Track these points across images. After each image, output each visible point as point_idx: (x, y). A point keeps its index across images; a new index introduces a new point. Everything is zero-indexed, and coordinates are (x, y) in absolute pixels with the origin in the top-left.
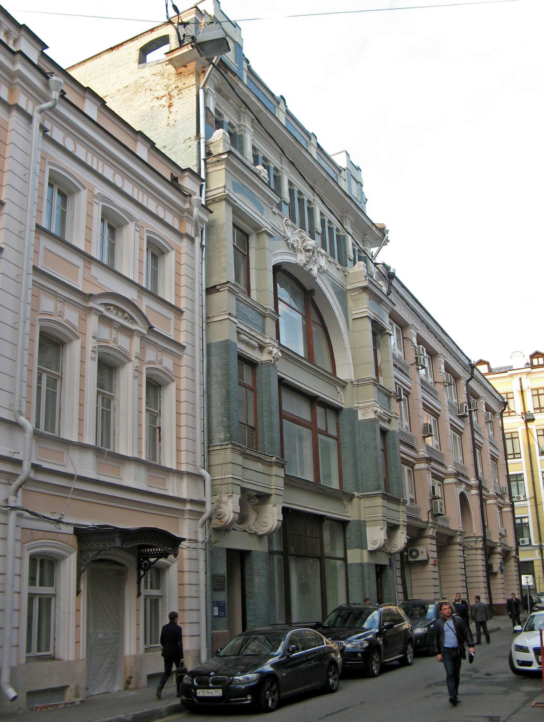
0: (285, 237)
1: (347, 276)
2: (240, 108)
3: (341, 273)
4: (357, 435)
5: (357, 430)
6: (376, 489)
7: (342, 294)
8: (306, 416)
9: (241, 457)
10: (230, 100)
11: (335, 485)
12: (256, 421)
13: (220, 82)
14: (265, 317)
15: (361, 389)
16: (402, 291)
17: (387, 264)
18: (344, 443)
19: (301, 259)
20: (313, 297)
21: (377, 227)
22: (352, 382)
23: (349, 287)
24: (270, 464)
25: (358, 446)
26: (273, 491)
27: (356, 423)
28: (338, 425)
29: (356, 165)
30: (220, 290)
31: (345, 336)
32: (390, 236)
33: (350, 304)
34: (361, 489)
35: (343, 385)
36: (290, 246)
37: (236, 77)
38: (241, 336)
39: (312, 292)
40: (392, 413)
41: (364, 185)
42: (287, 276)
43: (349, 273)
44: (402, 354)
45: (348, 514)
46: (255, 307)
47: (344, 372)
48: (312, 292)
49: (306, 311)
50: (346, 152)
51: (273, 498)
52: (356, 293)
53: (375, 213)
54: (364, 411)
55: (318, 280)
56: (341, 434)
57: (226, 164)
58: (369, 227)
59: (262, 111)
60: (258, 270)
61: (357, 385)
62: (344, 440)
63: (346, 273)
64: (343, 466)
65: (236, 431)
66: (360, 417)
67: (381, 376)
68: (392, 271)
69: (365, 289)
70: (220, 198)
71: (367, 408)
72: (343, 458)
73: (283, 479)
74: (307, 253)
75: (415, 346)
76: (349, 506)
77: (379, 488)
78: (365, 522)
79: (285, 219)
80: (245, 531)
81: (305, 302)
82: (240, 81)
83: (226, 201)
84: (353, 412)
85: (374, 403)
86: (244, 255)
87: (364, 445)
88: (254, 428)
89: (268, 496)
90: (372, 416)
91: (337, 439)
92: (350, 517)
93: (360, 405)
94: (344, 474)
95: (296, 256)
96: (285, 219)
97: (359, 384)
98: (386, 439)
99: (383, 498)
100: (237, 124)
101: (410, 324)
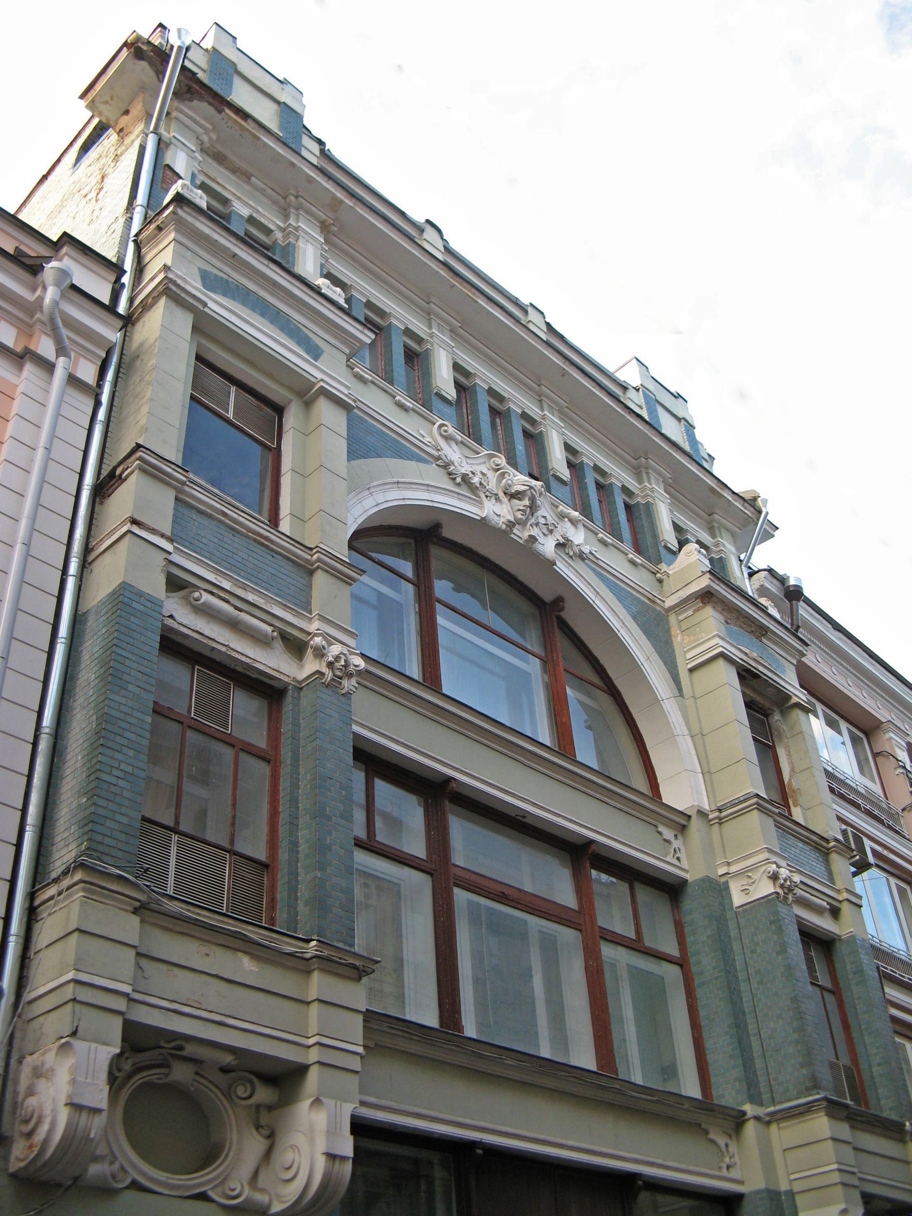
0: (438, 458)
1: (665, 583)
2: (285, 198)
3: (646, 575)
4: (736, 947)
5: (734, 933)
6: (807, 1089)
7: (655, 623)
8: (564, 893)
9: (136, 920)
10: (253, 179)
11: (691, 1088)
12: (273, 844)
13: (214, 136)
14: (311, 573)
15: (728, 827)
16: (839, 639)
17: (781, 571)
18: (701, 973)
19: (498, 512)
20: (562, 614)
21: (734, 493)
22: (701, 813)
23: (670, 602)
24: (302, 966)
25: (741, 976)
26: (313, 1055)
27: (729, 915)
28: (679, 927)
29: (672, 391)
30: (123, 476)
31: (671, 707)
32: (773, 512)
33: (678, 639)
34: (766, 1096)
35: (681, 823)
36: (459, 480)
37: (249, 121)
38: (196, 595)
39: (558, 602)
40: (838, 891)
41: (695, 424)
42: (477, 563)
43: (668, 575)
44: (877, 789)
45: (735, 1174)
46: (267, 538)
47: (682, 790)
48: (558, 602)
49: (546, 648)
50: (637, 359)
51: (313, 1075)
52: (690, 612)
53: (734, 471)
54: (745, 881)
55: (562, 567)
56: (690, 950)
57: (176, 230)
58: (712, 490)
59: (341, 201)
60: (300, 474)
61: (721, 821)
62: (699, 962)
63: (658, 575)
64: (705, 1035)
65: (122, 837)
66: (738, 899)
67: (795, 806)
68: (792, 582)
69: (706, 596)
70: (155, 294)
71: (750, 870)
72: (702, 1013)
73: (360, 1018)
74: (515, 501)
75: (904, 768)
76: (733, 1148)
77: (816, 1086)
78: (791, 1194)
79: (437, 424)
80: (203, 1197)
81: (542, 625)
82: (262, 131)
83: (168, 296)
84: (718, 889)
85: (766, 855)
86: (269, 449)
87: (758, 972)
88: (266, 866)
89: (301, 1070)
90: (766, 888)
91: (682, 963)
92: (741, 1182)
93: (734, 869)
94: (710, 1057)
95: (480, 504)
96: (437, 424)
97: (720, 816)
98: (836, 959)
99: (830, 1115)
100: (279, 227)
101: (884, 721)
